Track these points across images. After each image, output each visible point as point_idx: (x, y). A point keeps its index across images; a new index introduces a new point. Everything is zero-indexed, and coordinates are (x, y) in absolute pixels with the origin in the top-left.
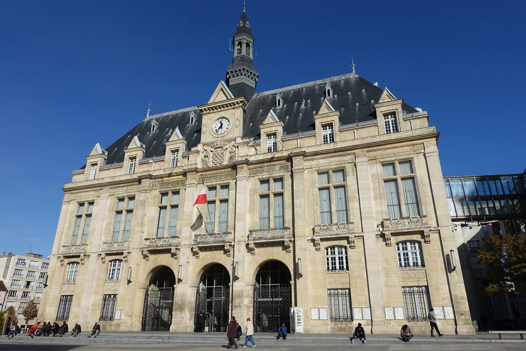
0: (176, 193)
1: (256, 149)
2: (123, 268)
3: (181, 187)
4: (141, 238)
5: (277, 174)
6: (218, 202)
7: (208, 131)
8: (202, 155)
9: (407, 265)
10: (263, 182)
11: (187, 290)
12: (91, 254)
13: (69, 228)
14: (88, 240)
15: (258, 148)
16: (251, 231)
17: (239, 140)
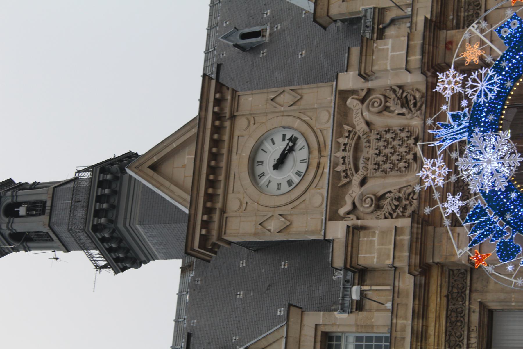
1: (393, 21)
3: (477, 297)
15: (389, 16)
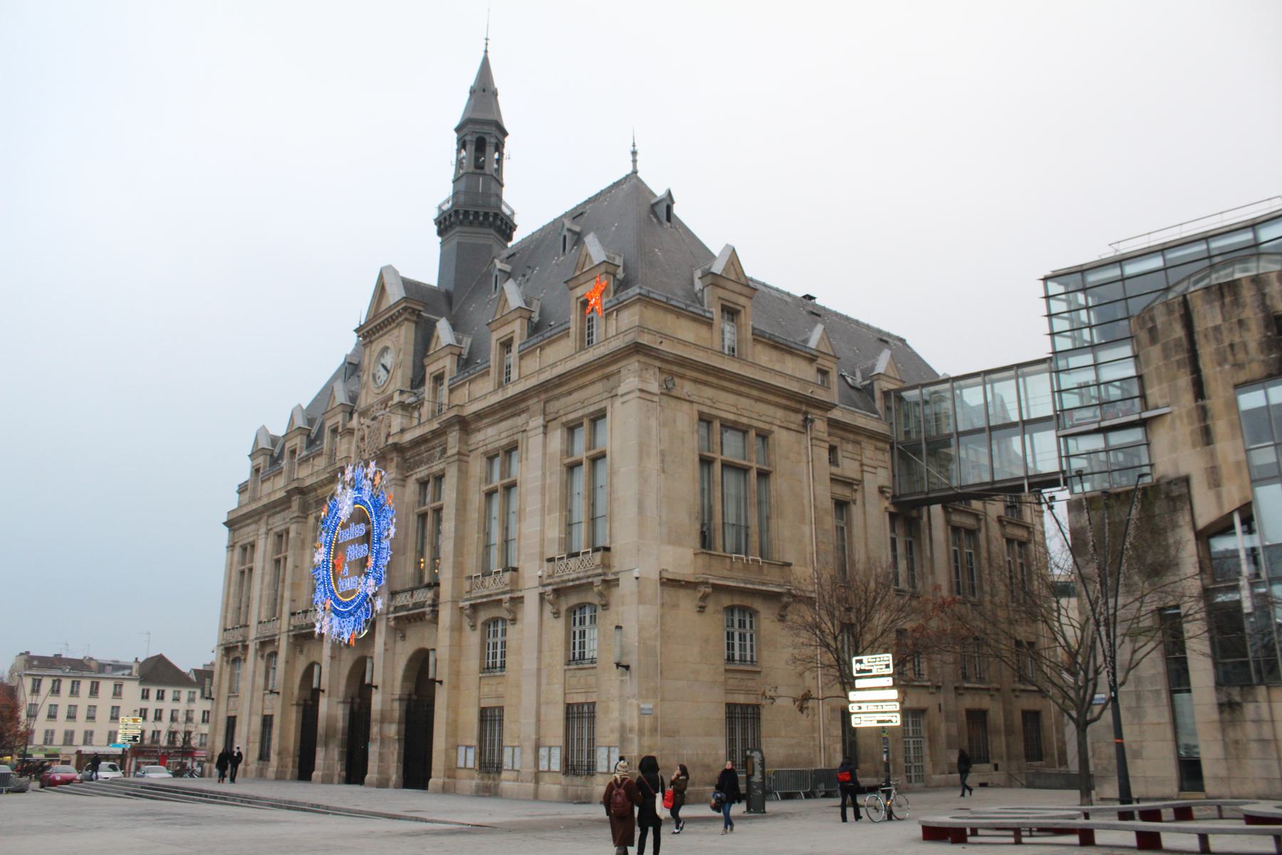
5: (437, 467)
11: (331, 710)
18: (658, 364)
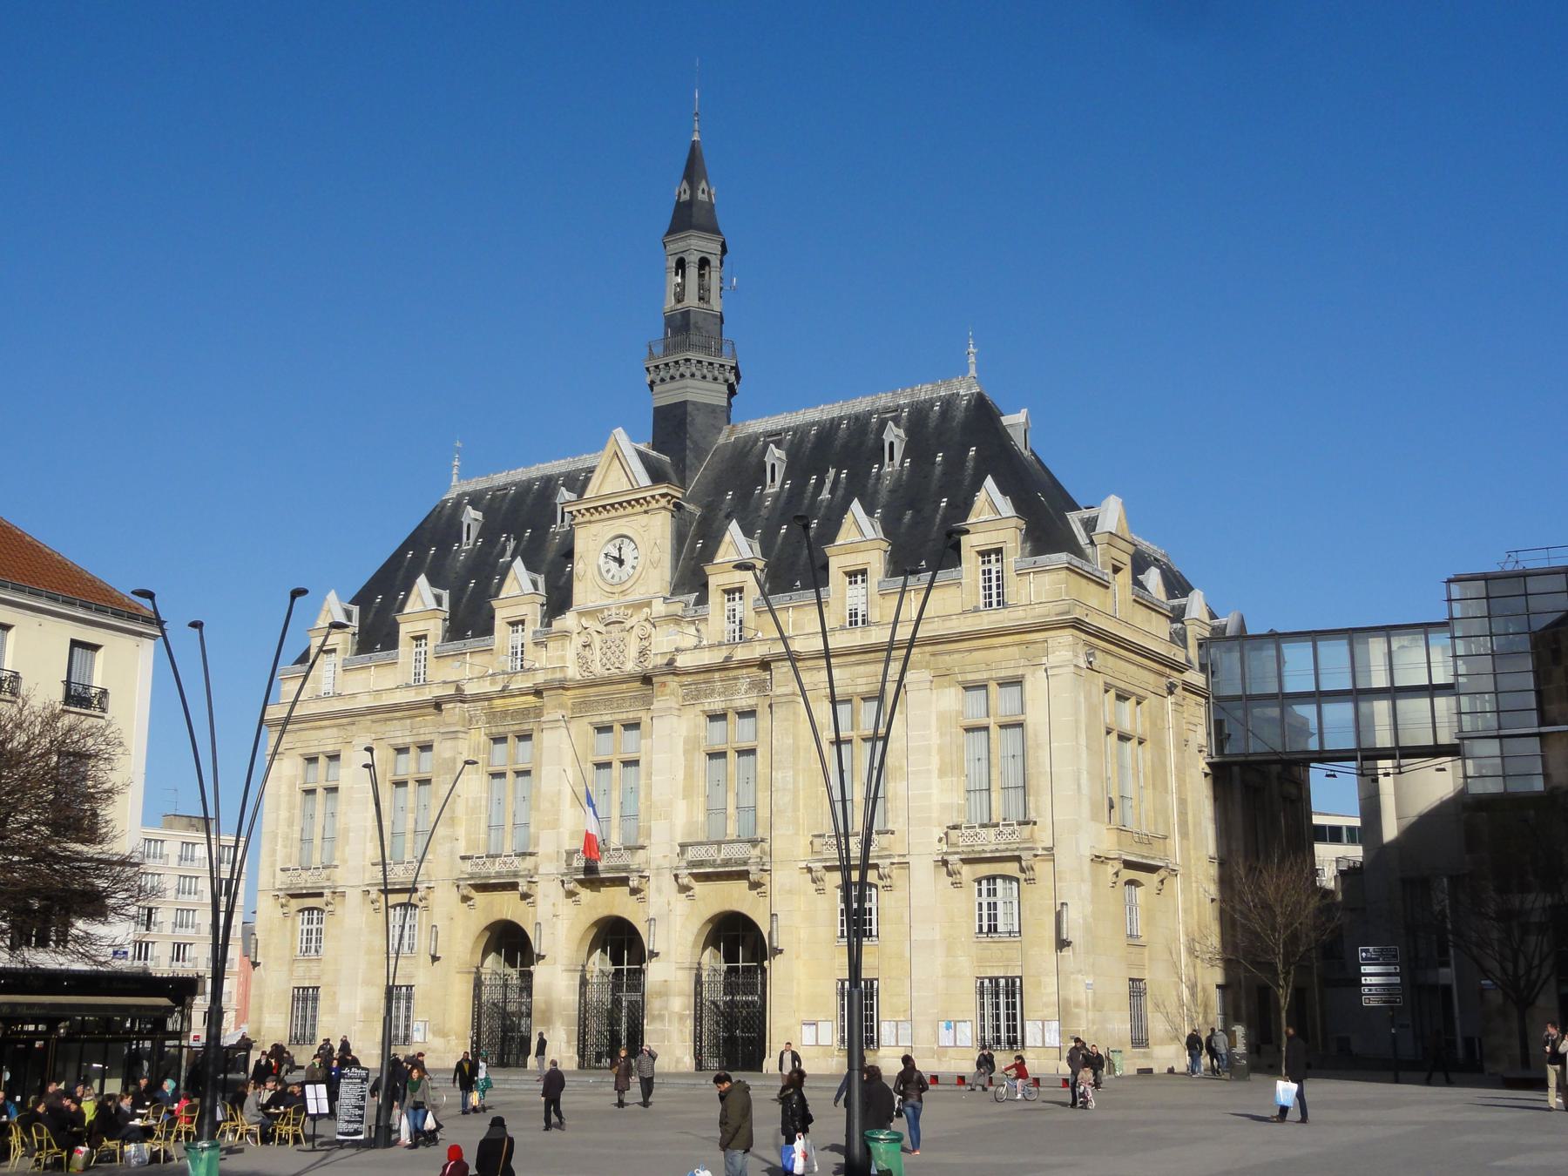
0: (525, 737)
2: (420, 923)
4: (452, 853)
5: (744, 701)
6: (617, 765)
7: (589, 575)
8: (577, 641)
9: (993, 929)
10: (713, 717)
12: (348, 891)
13: (291, 824)
14: (338, 854)
16: (683, 846)
17: (659, 608)
18: (1083, 636)
